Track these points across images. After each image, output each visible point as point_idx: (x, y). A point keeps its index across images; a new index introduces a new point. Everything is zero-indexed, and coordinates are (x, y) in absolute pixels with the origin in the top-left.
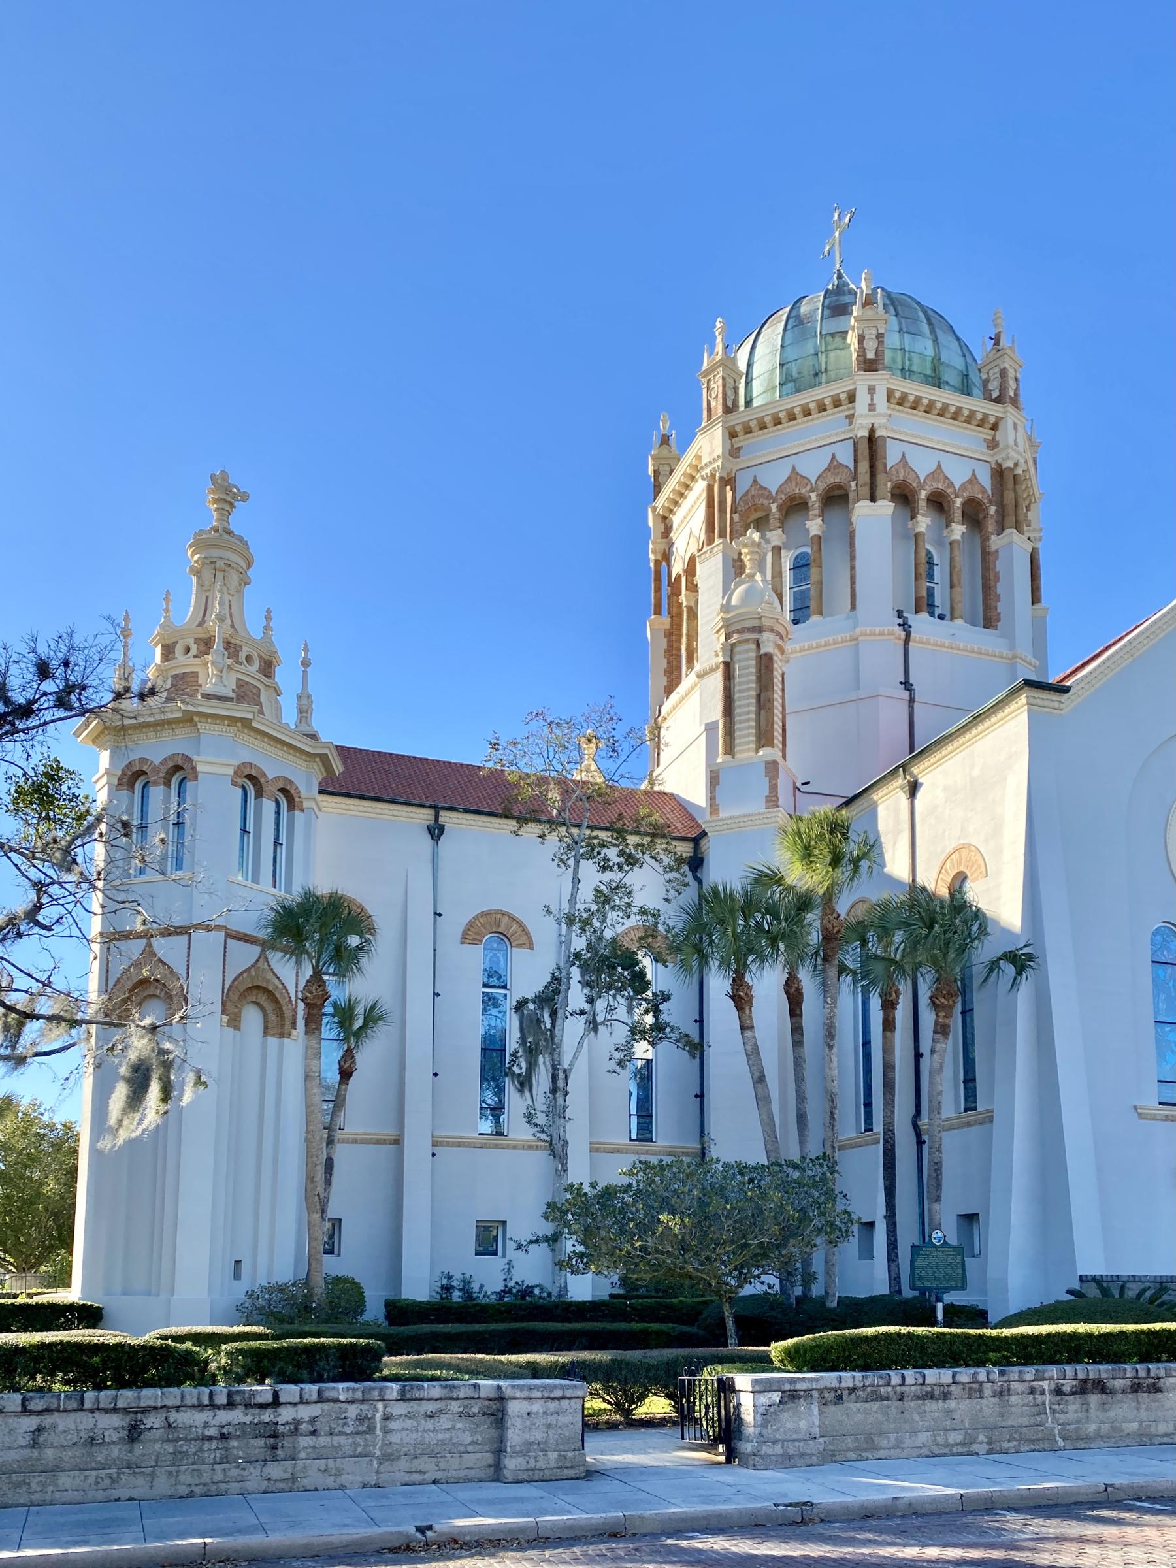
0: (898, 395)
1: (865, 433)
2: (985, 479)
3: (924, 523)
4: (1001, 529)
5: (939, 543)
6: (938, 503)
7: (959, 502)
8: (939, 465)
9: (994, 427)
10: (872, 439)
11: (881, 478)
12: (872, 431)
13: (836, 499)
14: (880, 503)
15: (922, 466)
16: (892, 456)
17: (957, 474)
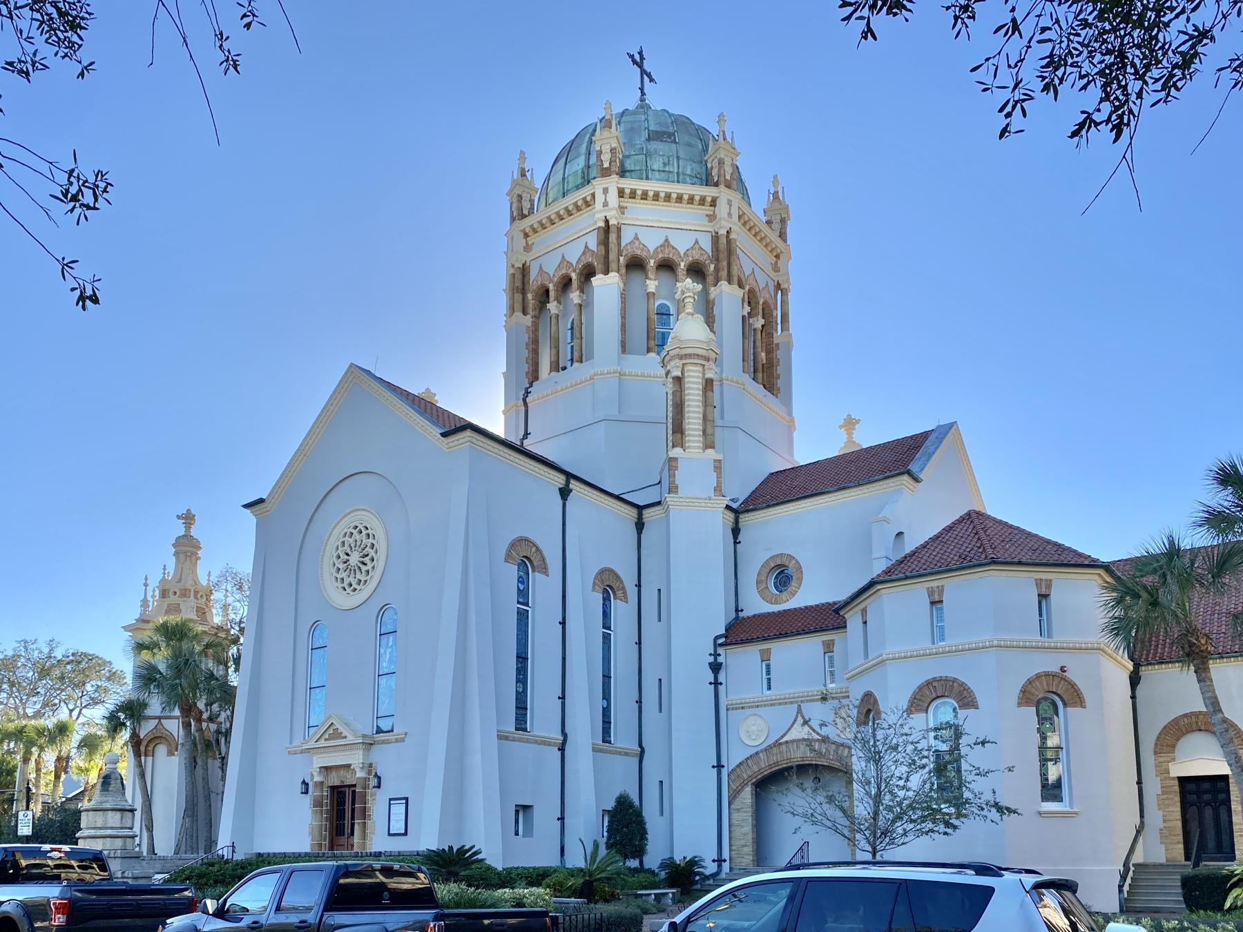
0: (627, 191)
1: (602, 224)
2: (707, 245)
3: (652, 285)
4: (717, 281)
5: (671, 296)
6: (667, 266)
7: (682, 264)
8: (667, 240)
9: (714, 203)
10: (607, 228)
11: (612, 256)
12: (607, 221)
13: (588, 273)
14: (611, 274)
15: (651, 242)
16: (627, 237)
17: (682, 244)
